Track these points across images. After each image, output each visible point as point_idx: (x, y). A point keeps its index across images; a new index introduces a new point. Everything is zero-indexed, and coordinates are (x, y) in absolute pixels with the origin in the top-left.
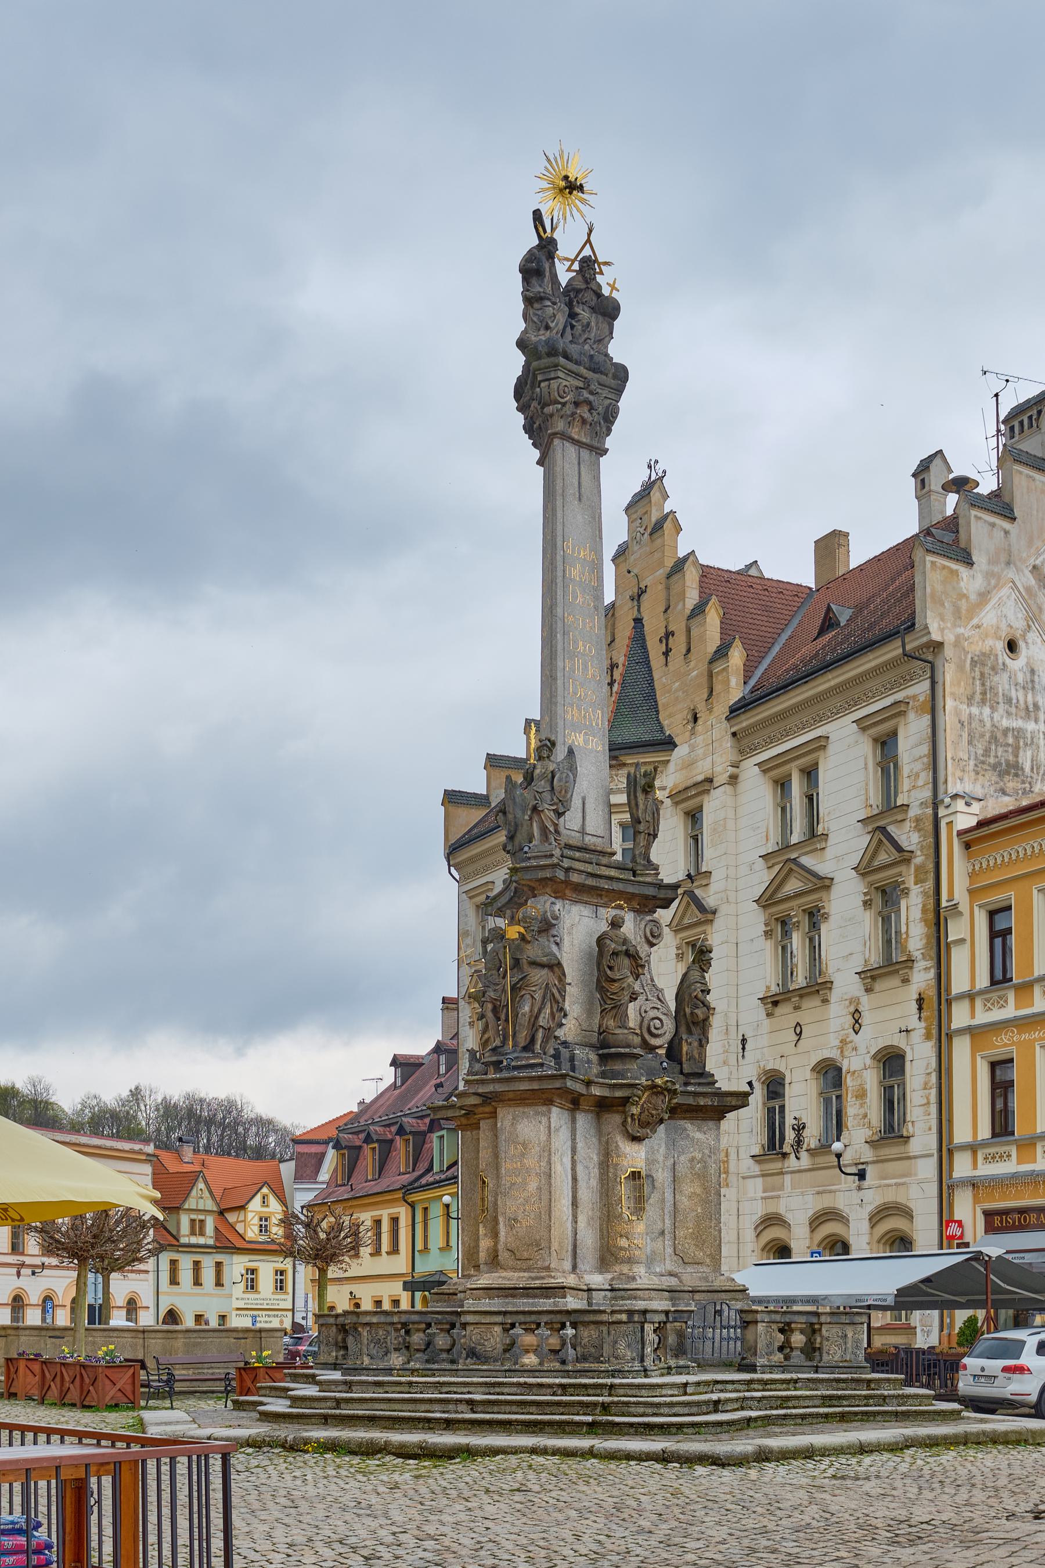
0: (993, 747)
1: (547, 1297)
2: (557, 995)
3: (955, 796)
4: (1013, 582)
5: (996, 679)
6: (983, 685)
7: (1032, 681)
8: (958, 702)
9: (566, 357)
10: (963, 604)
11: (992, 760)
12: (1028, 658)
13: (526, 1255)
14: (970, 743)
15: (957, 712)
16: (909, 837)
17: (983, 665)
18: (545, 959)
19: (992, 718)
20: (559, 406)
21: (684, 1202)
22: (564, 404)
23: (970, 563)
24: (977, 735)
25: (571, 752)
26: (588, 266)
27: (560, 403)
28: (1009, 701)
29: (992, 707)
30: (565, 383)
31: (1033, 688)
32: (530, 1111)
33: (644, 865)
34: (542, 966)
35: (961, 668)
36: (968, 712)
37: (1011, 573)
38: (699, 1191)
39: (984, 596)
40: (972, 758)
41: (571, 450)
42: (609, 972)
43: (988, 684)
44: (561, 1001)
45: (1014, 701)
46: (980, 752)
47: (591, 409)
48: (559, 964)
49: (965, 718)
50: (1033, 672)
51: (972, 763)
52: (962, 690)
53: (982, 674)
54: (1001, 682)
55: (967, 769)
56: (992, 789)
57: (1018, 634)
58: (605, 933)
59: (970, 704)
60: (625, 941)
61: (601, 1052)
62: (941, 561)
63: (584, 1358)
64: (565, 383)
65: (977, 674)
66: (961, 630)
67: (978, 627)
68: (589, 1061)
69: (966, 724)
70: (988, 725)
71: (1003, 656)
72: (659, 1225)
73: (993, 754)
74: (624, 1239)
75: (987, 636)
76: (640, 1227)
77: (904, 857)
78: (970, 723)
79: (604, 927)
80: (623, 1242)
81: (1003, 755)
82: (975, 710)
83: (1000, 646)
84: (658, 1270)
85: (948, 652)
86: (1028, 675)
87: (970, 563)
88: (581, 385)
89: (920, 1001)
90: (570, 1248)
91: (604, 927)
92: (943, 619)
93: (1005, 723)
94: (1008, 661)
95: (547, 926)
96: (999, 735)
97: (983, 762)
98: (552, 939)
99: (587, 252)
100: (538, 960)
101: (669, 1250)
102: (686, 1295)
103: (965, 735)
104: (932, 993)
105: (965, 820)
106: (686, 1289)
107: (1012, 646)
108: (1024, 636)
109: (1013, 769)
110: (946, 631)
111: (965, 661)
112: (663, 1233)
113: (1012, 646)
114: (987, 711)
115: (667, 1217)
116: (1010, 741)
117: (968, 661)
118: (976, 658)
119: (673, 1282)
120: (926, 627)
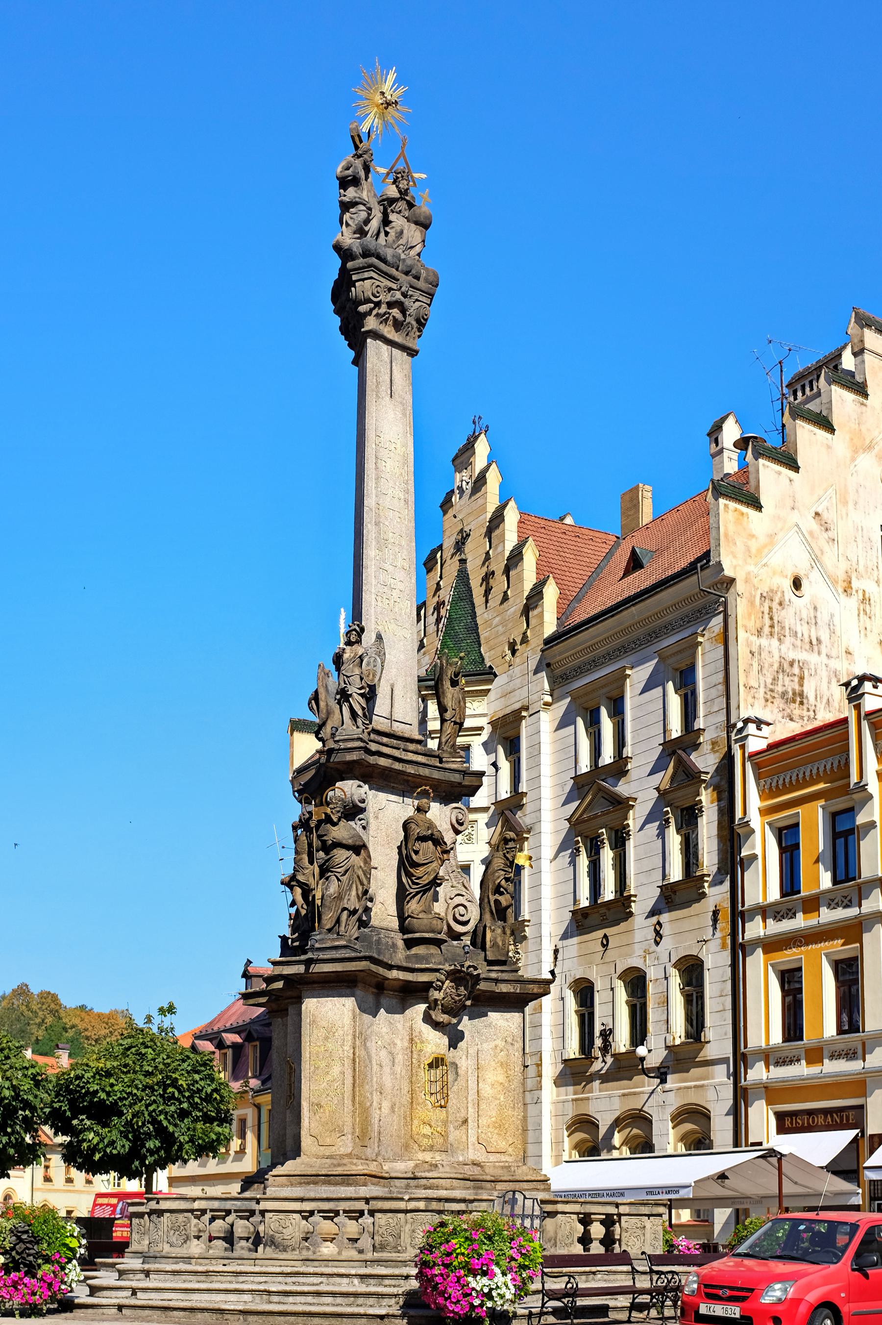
0: (781, 676)
1: (349, 1185)
2: (362, 877)
3: (746, 721)
4: (797, 526)
5: (783, 613)
6: (771, 619)
8: (749, 634)
9: (379, 257)
10: (754, 545)
11: (779, 689)
13: (328, 1141)
14: (760, 671)
15: (748, 644)
16: (705, 761)
18: (350, 841)
20: (372, 305)
21: (487, 1090)
22: (378, 304)
23: (758, 507)
24: (766, 665)
25: (379, 637)
27: (372, 302)
29: (780, 640)
30: (378, 283)
31: (816, 623)
33: (450, 753)
34: (347, 847)
35: (752, 603)
36: (758, 644)
37: (795, 517)
38: (501, 1078)
40: (762, 685)
41: (385, 348)
42: (414, 857)
43: (776, 619)
44: (365, 882)
45: (799, 635)
46: (769, 681)
47: (403, 311)
48: (364, 846)
50: (815, 608)
51: (762, 690)
52: (752, 623)
53: (770, 608)
54: (787, 617)
55: (756, 695)
56: (780, 715)
58: (410, 818)
60: (431, 825)
61: (406, 937)
62: (732, 505)
63: (383, 1247)
64: (378, 283)
65: (766, 610)
66: (751, 568)
68: (394, 946)
69: (756, 654)
71: (789, 594)
73: (780, 683)
74: (428, 1127)
75: (774, 573)
79: (410, 812)
81: (789, 684)
82: (764, 641)
83: (788, 583)
84: (461, 1159)
85: (740, 586)
86: (812, 611)
87: (758, 507)
88: (394, 286)
89: (715, 913)
91: (410, 812)
92: (735, 557)
93: (791, 655)
95: (353, 811)
96: (786, 666)
97: (772, 691)
98: (359, 823)
100: (344, 842)
101: (472, 1139)
102: (488, 1185)
103: (755, 665)
104: (727, 904)
105: (755, 744)
106: (489, 1178)
107: (797, 584)
109: (799, 697)
110: (737, 568)
111: (755, 597)
112: (465, 1121)
113: (797, 584)
114: (775, 642)
115: (470, 1105)
116: (796, 670)
118: (765, 594)
119: (477, 1170)
120: (719, 564)
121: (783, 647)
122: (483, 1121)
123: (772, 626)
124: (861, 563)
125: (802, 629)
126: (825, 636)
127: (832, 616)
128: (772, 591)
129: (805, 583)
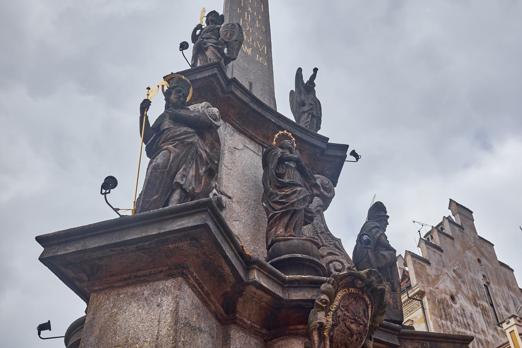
4: (447, 273)
5: (450, 310)
6: (445, 312)
7: (464, 314)
8: (436, 317)
12: (461, 304)
17: (443, 304)
19: (452, 326)
28: (457, 320)
29: (450, 322)
31: (465, 317)
49: (440, 324)
50: (463, 310)
52: (437, 312)
53: (443, 307)
57: (454, 294)
59: (441, 319)
65: (441, 307)
67: (437, 288)
70: (451, 329)
71: (450, 302)
75: (442, 292)
78: (443, 327)
82: (444, 322)
83: (448, 297)
94: (453, 304)
107: (453, 298)
108: (456, 295)
113: (453, 298)
114: (449, 323)
117: (437, 301)
121: (453, 325)
123: (446, 315)
124: (478, 293)
125: (459, 318)
126: (471, 322)
127: (472, 314)
128: (442, 300)
129: (456, 298)
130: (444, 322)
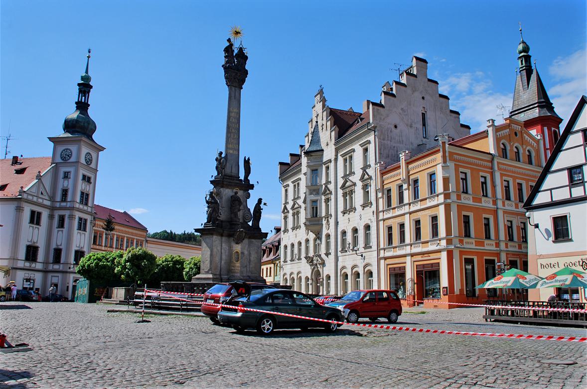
26: (241, 50)
32: (208, 236)
39: (388, 116)
72: (245, 264)
75: (389, 124)
76: (238, 264)
77: (370, 178)
80: (233, 268)
90: (219, 269)
93: (394, 145)
99: (241, 46)
107: (396, 127)
112: (246, 266)
113: (396, 127)
114: (389, 142)
122: (251, 266)
129: (398, 126)
130: (386, 142)
